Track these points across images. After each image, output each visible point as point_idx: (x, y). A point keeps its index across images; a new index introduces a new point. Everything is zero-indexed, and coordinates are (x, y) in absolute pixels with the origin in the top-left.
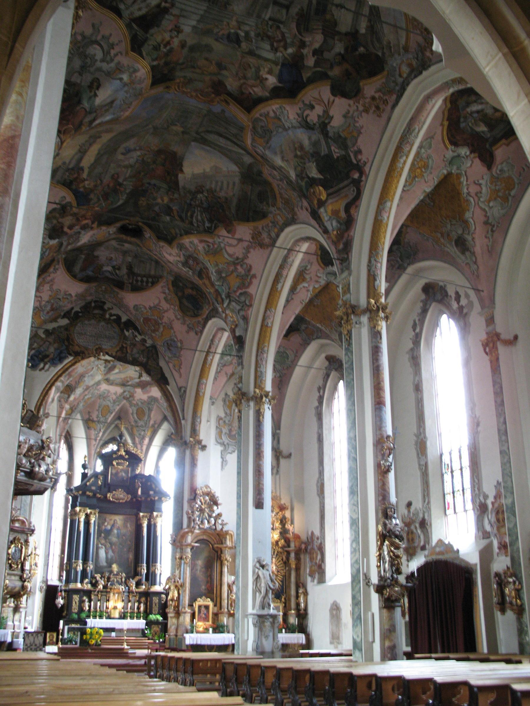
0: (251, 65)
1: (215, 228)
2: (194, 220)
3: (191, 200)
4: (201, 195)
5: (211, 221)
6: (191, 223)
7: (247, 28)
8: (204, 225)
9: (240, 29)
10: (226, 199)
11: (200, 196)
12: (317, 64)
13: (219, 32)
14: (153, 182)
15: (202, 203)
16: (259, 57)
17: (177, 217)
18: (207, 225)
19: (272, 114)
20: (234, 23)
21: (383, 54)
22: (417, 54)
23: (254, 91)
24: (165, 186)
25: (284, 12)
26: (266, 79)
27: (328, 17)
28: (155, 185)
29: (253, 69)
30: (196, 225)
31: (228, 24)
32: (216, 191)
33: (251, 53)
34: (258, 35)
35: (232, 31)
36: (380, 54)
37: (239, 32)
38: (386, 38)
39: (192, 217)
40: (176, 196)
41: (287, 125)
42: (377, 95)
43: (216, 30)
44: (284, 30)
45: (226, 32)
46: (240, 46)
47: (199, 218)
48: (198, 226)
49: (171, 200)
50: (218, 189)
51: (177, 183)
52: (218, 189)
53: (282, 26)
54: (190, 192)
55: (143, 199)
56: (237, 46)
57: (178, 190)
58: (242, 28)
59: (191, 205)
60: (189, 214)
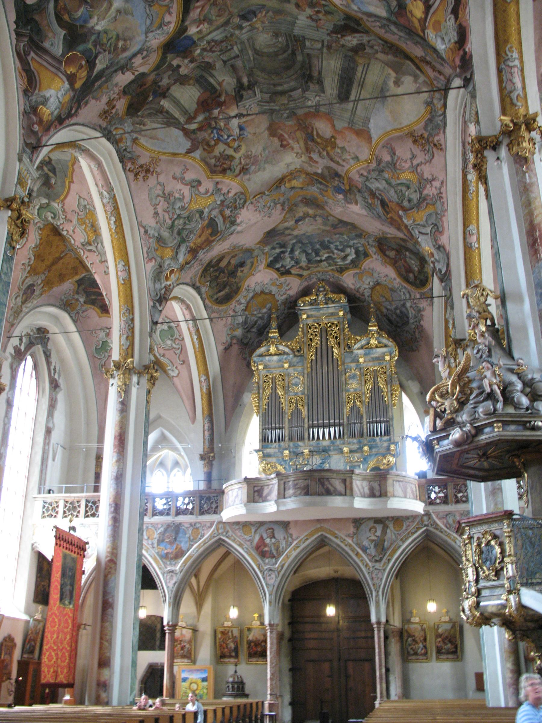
0: (218, 18)
7: (244, 31)
9: (250, 25)
12: (171, 65)
13: (266, 13)
16: (217, 28)
19: (167, 18)
20: (258, 25)
21: (138, 116)
22: (129, 152)
23: (198, 7)
25: (225, 59)
26: (198, 27)
27: (191, 82)
29: (214, 18)
31: (263, 22)
33: (227, 23)
34: (232, 35)
35: (255, 20)
36: (139, 113)
37: (249, 23)
38: (149, 122)
41: (150, 35)
42: (114, 111)
43: (270, 14)
44: (215, 54)
45: (259, 15)
46: (239, 16)
53: (219, 53)
56: (241, 14)
58: (248, 28)
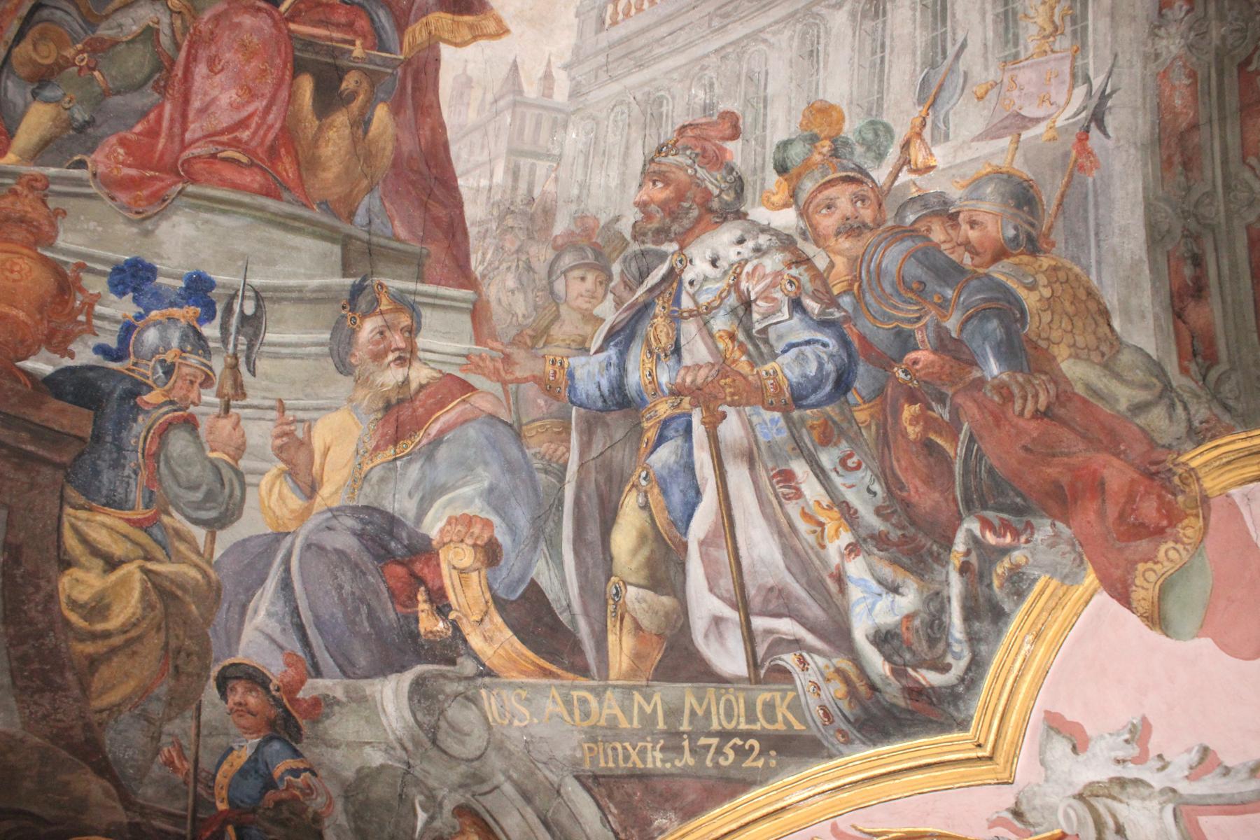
1: (987, 613)
2: (705, 604)
3: (623, 335)
4: (723, 241)
5: (911, 543)
6: (678, 659)
8: (837, 634)
10: (1023, 197)
11: (710, 257)
14: (181, 242)
15: (759, 344)
17: (492, 640)
18: (875, 604)
24: (305, 263)
28: (198, 289)
30: (729, 658)
32: (878, 134)
39: (665, 568)
40: (444, 340)
47: (759, 545)
48: (766, 670)
49: (400, 419)
50: (901, 113)
51: (428, 177)
52: (901, 113)
54: (593, 248)
55: (103, 527)
57: (462, 274)
59: (621, 401)
60: (624, 539)
